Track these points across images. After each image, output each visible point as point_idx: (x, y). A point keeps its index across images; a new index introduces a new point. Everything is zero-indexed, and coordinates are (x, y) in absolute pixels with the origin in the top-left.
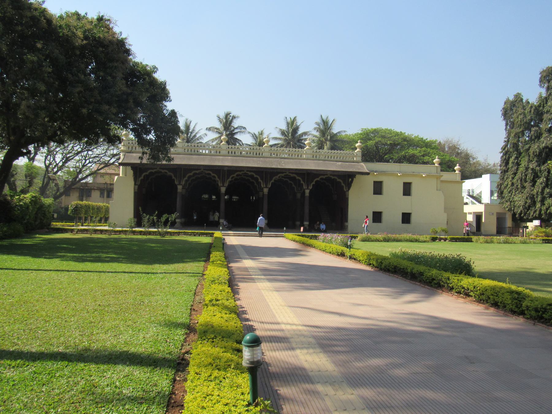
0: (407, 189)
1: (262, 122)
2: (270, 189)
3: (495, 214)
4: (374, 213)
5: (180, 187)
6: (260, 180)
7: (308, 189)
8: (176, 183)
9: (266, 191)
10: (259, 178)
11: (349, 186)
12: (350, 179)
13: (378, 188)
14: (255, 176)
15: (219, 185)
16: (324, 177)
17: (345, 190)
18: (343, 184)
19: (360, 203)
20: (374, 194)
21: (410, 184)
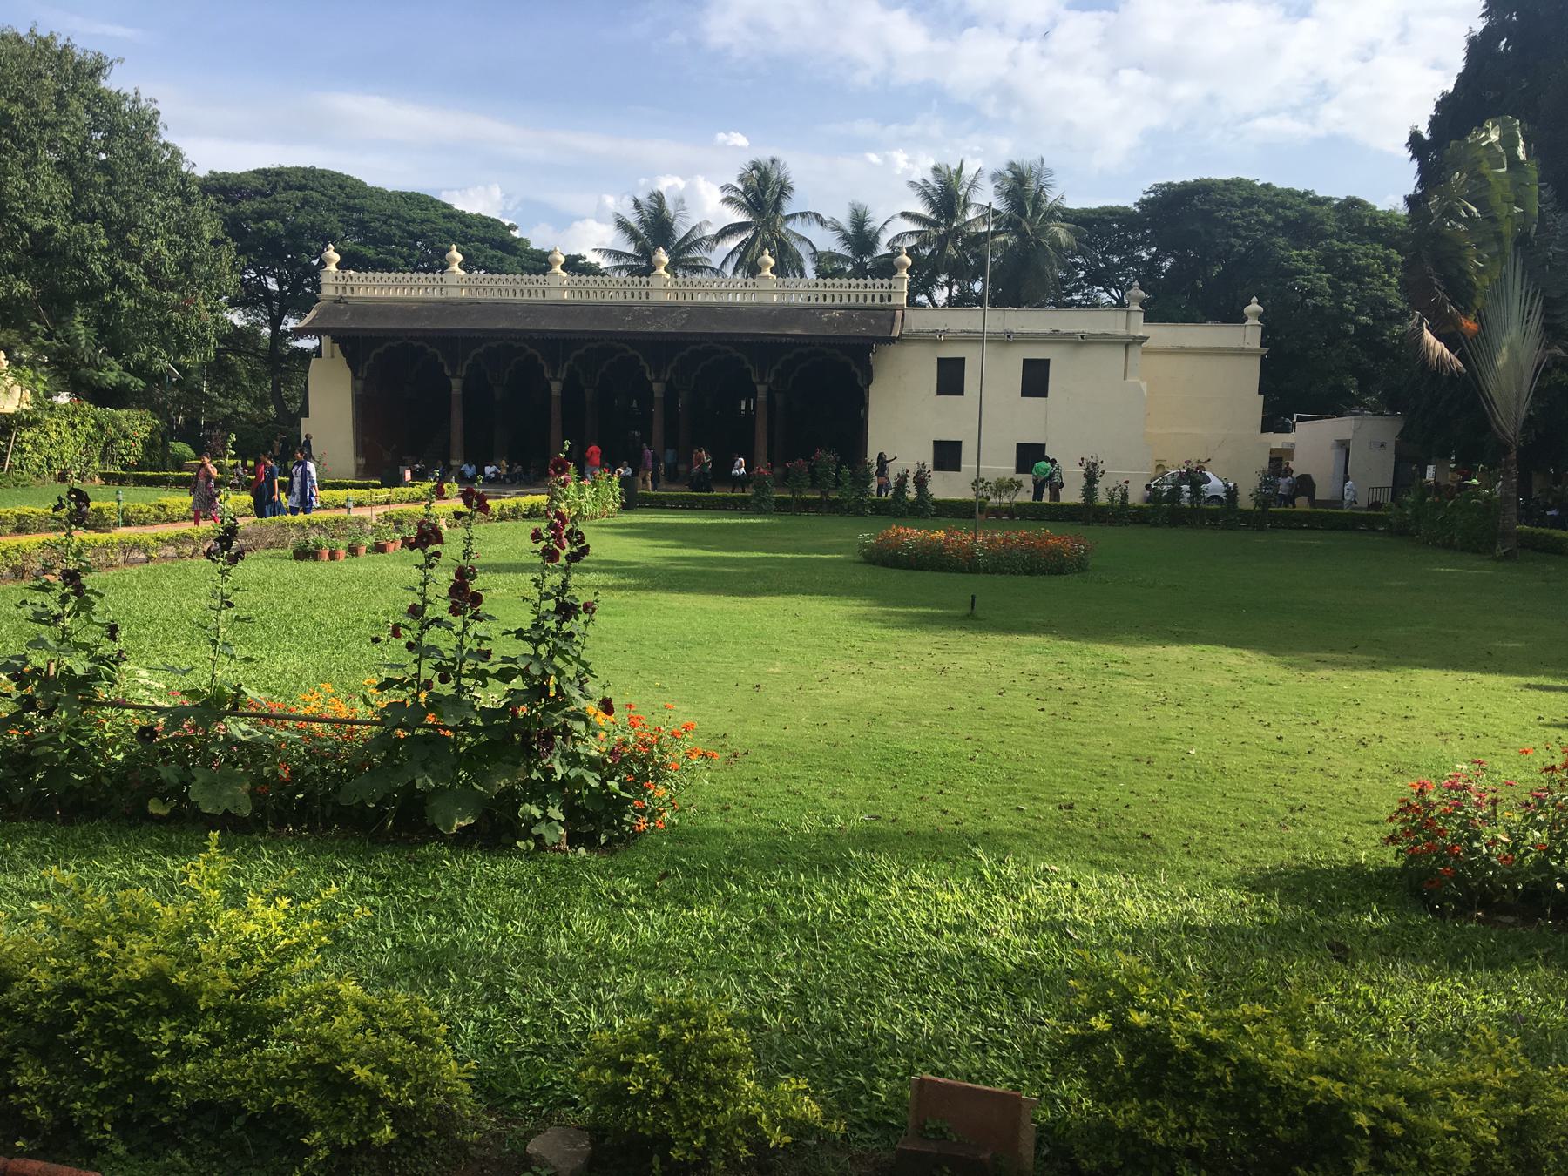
0: (1035, 380)
4: (938, 445)
5: (456, 384)
13: (951, 379)
19: (902, 423)
20: (940, 392)
21: (1045, 363)
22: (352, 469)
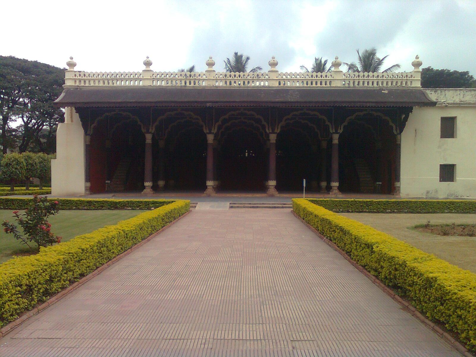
2: (279, 135)
5: (149, 138)
6: (264, 123)
7: (336, 132)
8: (144, 130)
9: (273, 138)
10: (263, 120)
11: (402, 126)
12: (404, 116)
13: (448, 128)
15: (205, 131)
16: (362, 114)
17: (395, 133)
18: (391, 124)
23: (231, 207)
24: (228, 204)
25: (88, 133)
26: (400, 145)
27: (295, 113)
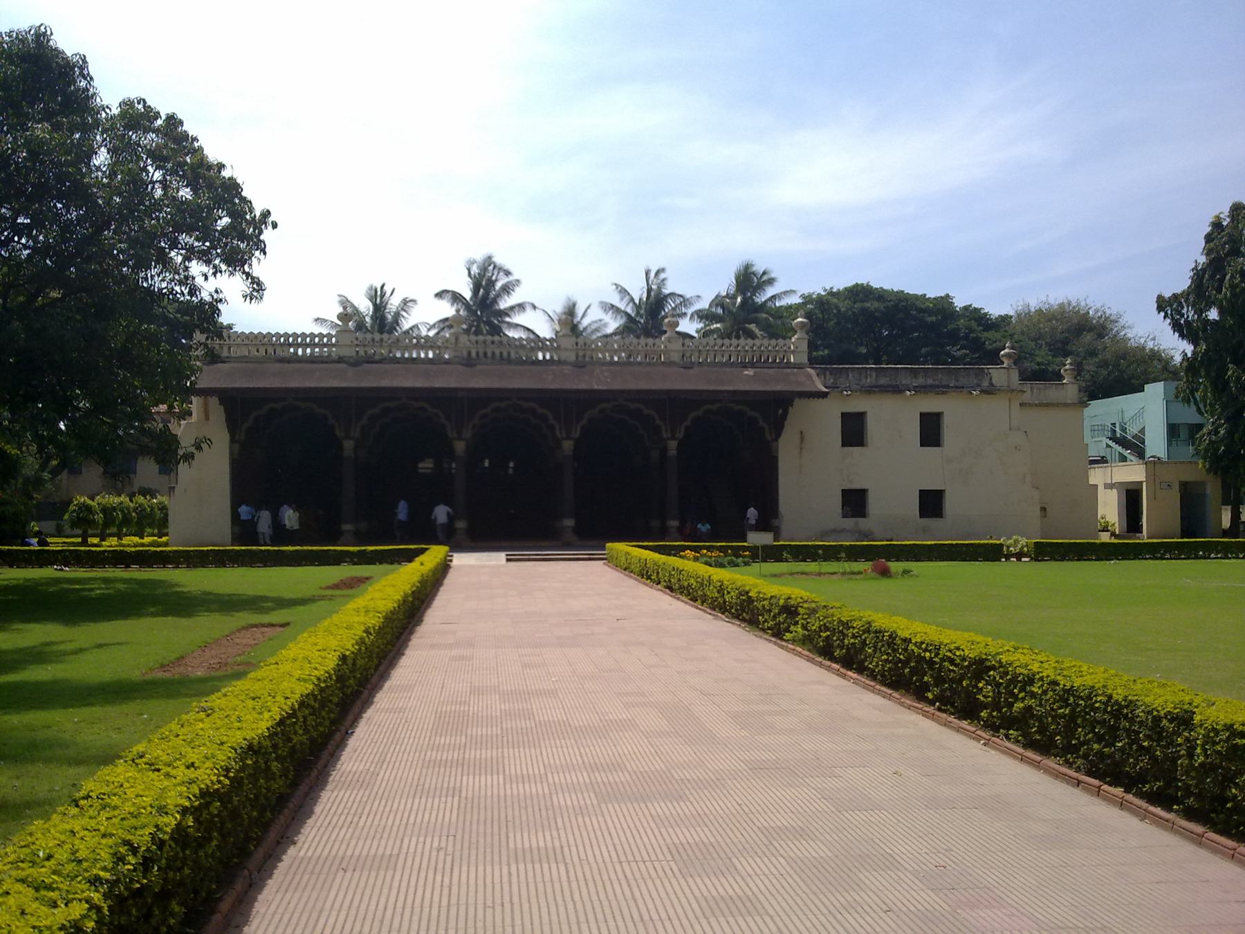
0: (931, 430)
1: (568, 280)
3: (1177, 487)
5: (348, 445)
6: (552, 421)
7: (673, 438)
9: (568, 446)
10: (550, 416)
11: (778, 427)
13: (854, 431)
14: (540, 410)
15: (450, 436)
16: (714, 407)
18: (761, 423)
21: (938, 416)
22: (229, 539)
23: (508, 560)
24: (501, 557)
25: (237, 438)
26: (776, 458)
27: (604, 405)
